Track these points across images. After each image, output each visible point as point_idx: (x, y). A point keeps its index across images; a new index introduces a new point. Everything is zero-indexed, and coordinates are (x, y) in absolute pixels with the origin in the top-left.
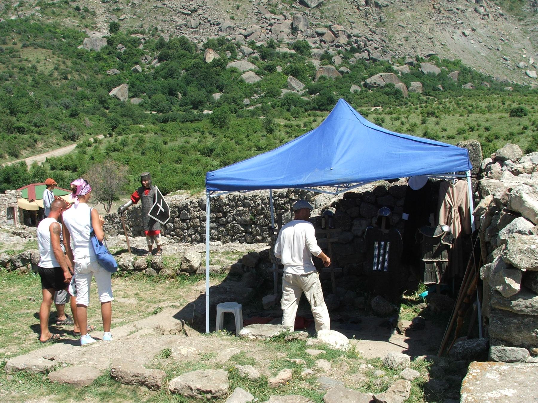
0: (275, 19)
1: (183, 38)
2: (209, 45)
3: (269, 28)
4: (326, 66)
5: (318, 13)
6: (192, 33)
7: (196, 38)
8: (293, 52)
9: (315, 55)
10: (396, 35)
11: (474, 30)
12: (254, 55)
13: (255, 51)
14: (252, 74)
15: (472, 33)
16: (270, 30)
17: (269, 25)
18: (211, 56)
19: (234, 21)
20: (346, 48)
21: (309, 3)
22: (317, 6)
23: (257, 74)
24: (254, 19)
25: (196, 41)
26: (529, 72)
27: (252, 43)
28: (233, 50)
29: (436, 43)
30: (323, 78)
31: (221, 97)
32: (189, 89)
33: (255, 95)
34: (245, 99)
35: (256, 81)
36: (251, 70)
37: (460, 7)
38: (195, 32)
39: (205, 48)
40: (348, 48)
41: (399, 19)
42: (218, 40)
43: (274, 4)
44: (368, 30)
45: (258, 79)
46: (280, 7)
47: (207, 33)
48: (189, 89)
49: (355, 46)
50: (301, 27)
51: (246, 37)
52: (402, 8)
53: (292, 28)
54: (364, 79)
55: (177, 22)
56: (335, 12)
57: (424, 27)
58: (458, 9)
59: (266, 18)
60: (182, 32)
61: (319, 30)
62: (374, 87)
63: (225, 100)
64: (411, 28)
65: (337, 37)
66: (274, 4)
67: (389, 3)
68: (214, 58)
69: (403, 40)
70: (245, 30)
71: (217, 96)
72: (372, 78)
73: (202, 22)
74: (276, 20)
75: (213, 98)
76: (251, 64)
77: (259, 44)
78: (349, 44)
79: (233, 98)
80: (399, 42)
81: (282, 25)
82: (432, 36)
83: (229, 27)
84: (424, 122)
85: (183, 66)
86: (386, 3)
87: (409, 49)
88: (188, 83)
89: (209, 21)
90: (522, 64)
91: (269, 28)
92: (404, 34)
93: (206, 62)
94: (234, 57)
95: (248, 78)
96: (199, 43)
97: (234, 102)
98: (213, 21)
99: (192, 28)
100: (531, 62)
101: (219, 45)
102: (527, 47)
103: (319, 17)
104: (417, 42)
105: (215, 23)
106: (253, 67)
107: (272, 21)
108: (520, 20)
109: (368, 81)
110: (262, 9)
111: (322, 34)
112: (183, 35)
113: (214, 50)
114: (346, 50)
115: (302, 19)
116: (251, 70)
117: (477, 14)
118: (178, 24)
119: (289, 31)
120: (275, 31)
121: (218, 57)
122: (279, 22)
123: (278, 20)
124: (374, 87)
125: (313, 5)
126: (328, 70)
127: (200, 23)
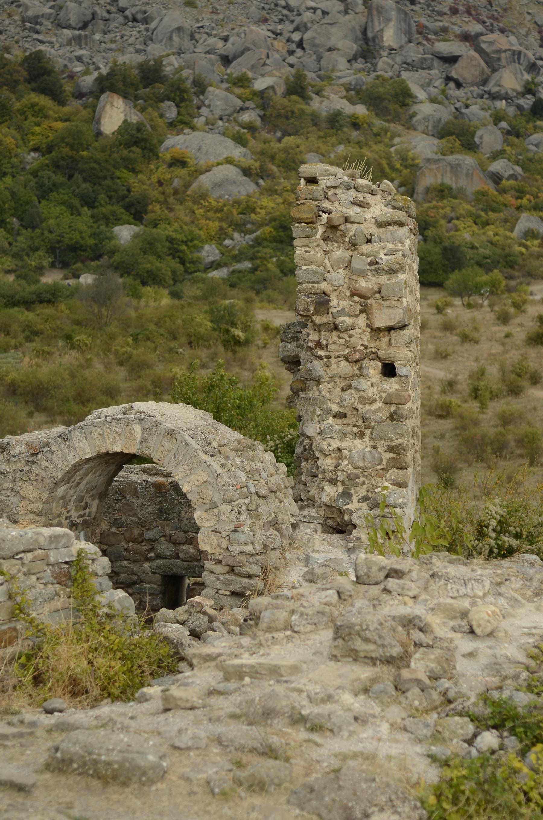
0: (315, 10)
1: (38, 56)
2: (112, 83)
3: (296, 37)
4: (450, 158)
6: (69, 43)
7: (79, 59)
8: (361, 110)
9: (426, 119)
13: (248, 104)
14: (231, 171)
16: (300, 44)
17: (297, 29)
18: (115, 115)
19: (195, 11)
20: (522, 102)
23: (246, 172)
24: (253, 9)
25: (78, 68)
27: (242, 82)
28: (183, 100)
31: (136, 236)
32: (44, 208)
33: (236, 235)
34: (207, 247)
36: (229, 161)
38: (78, 40)
39: (102, 91)
40: (527, 102)
42: (142, 67)
45: (246, 188)
47: (113, 46)
48: (44, 208)
50: (390, 36)
51: (226, 60)
55: (27, 8)
60: (40, 37)
61: (445, 48)
63: (149, 246)
65: (494, 70)
68: (125, 121)
70: (226, 39)
71: (125, 233)
73: (101, 12)
74: (319, 12)
75: (111, 238)
76: (230, 143)
77: (260, 84)
78: (529, 89)
79: (171, 240)
81: (334, 30)
83: (179, 29)
85: (34, 141)
88: (44, 192)
89: (122, 10)
91: (296, 37)
93: (99, 134)
94: (187, 118)
95: (217, 185)
96: (87, 73)
97: (174, 252)
98: (134, 10)
99: (69, 27)
101: (145, 83)
103: (446, 10)
105: (139, 16)
106: (237, 152)
107: (307, 16)
111: (452, 60)
112: (42, 47)
113: (125, 97)
114: (520, 108)
116: (229, 161)
118: (30, 13)
120: (315, 45)
121: (134, 118)
122: (327, 20)
123: (325, 13)
126: (455, 168)
127: (94, 15)
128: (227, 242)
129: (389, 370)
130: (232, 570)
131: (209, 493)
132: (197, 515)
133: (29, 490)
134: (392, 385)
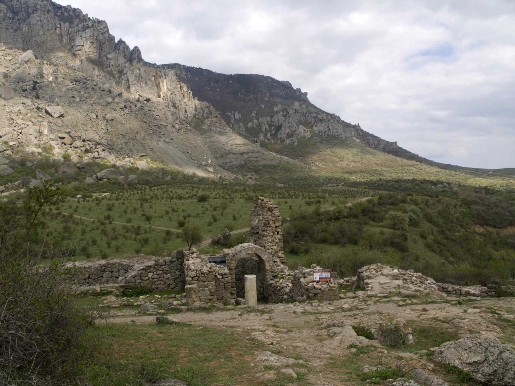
5: (60, 121)
10: (119, 141)
11: (172, 139)
12: (7, 152)
15: (171, 141)
17: (20, 129)
20: (82, 149)
21: (53, 114)
22: (59, 117)
26: (208, 168)
27: (6, 143)
29: (147, 147)
30: (64, 172)
33: (9, 184)
35: (10, 172)
36: (5, 164)
37: (163, 123)
41: (120, 130)
43: (24, 113)
44: (97, 137)
46: (29, 115)
49: (88, 148)
50: (46, 132)
52: (123, 122)
53: (40, 133)
54: (95, 173)
56: (73, 122)
57: (138, 136)
58: (161, 125)
59: (17, 123)
61: (61, 135)
62: (103, 178)
64: (129, 137)
65: (74, 141)
66: (24, 113)
67: (113, 118)
69: (123, 145)
72: (102, 172)
76: (5, 159)
77: (11, 143)
80: (120, 146)
81: (30, 130)
82: (143, 142)
84: (142, 206)
86: (111, 118)
87: (128, 151)
90: (204, 163)
91: (20, 131)
92: (125, 140)
100: (210, 161)
102: (206, 152)
104: (133, 146)
107: (23, 126)
108: (201, 134)
109: (99, 174)
110: (14, 116)
111: (63, 138)
114: (81, 150)
115: (47, 126)
116: (5, 164)
117: (174, 129)
119: (35, 134)
122: (28, 127)
124: (103, 178)
125: (56, 116)
128: (7, 185)
129: (278, 233)
130: (272, 272)
131: (268, 259)
132: (266, 263)
133: (233, 262)
134: (279, 236)
